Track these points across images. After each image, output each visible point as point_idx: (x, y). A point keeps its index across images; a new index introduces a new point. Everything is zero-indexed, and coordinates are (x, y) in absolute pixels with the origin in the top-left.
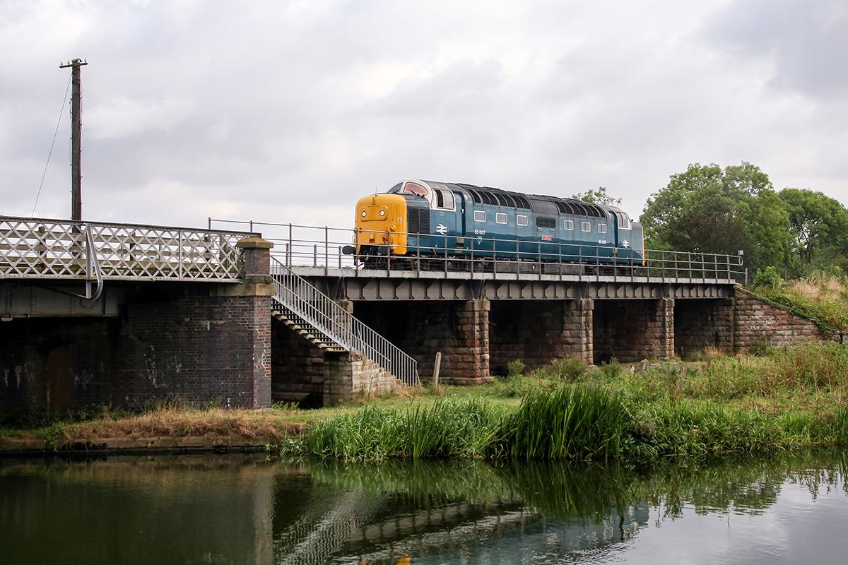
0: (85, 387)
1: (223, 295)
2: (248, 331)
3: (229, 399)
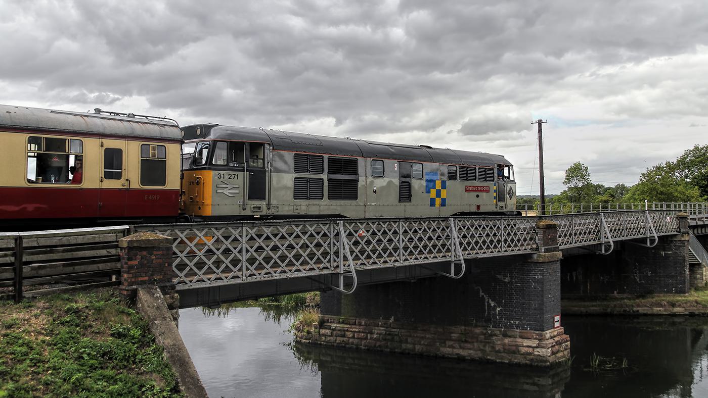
1: (671, 239)
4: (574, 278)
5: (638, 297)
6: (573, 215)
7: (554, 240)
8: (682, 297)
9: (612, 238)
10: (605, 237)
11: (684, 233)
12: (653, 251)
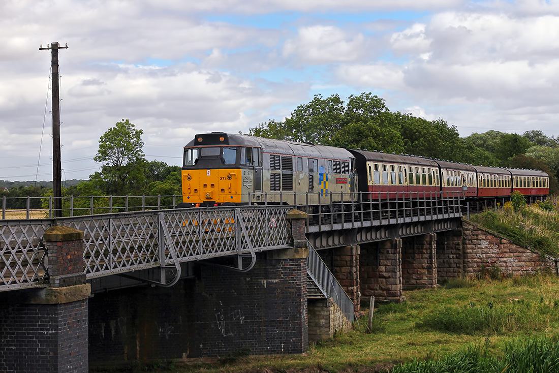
0: (167, 337)
1: (277, 258)
2: (296, 288)
3: (282, 345)
4: (113, 332)
5: (223, 363)
6: (110, 215)
7: (77, 263)
8: (295, 359)
9: (178, 257)
10: (167, 255)
11: (300, 246)
12: (248, 279)
